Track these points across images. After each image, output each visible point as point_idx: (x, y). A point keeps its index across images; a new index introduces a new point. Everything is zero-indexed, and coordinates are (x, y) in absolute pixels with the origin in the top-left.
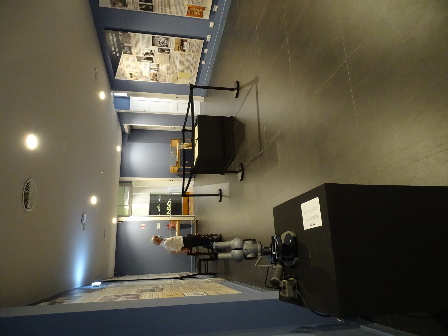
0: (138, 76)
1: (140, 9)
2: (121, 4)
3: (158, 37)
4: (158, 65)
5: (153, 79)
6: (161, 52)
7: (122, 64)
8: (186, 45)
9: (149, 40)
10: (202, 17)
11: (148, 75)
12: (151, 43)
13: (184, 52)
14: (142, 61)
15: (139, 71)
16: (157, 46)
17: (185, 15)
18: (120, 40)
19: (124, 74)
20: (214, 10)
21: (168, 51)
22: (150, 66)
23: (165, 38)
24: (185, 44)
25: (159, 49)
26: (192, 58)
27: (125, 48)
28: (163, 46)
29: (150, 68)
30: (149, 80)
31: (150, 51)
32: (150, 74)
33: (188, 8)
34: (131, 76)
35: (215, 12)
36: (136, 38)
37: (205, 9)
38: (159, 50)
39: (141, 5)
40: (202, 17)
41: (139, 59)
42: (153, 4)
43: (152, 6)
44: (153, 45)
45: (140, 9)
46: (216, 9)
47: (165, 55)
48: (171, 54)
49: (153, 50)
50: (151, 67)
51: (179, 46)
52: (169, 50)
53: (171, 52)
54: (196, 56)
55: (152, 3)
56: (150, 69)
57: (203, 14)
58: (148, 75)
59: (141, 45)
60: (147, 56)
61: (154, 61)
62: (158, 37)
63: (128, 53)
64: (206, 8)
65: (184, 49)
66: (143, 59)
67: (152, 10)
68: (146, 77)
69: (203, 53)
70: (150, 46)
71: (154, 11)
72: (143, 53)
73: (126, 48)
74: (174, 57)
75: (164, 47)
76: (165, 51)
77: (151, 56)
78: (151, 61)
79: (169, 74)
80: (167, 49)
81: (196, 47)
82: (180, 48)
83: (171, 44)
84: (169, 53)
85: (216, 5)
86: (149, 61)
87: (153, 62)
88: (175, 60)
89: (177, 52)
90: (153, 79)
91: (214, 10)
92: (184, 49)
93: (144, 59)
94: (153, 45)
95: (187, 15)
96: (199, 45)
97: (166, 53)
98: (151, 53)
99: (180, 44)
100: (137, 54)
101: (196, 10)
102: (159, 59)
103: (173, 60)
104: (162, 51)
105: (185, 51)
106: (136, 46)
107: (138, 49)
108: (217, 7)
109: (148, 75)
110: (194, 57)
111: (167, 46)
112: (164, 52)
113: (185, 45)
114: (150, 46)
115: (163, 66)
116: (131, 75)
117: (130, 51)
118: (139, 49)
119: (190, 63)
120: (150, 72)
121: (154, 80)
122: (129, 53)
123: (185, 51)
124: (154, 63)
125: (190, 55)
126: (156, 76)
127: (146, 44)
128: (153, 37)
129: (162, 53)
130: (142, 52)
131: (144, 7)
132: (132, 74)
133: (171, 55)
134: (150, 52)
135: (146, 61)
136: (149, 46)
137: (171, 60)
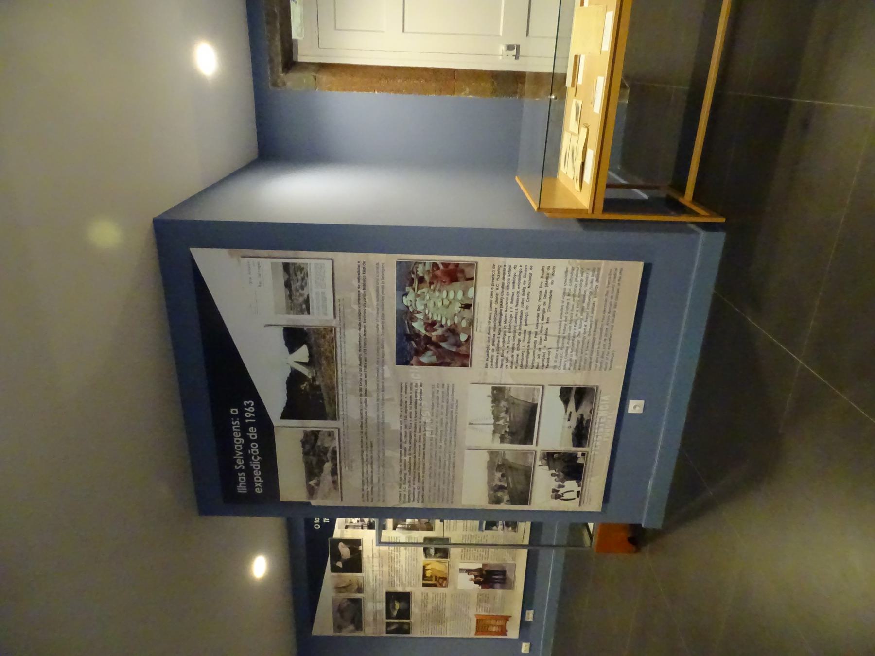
1: (388, 632)
2: (351, 627)
10: (506, 635)
17: (472, 634)
20: (527, 619)
33: (477, 620)
35: (530, 622)
37: (510, 619)
39: (388, 625)
40: (506, 635)
42: (412, 620)
43: (409, 624)
45: (388, 632)
46: (530, 616)
55: (408, 617)
57: (507, 629)
64: (510, 617)
67: (408, 632)
85: (531, 609)
91: (527, 619)
95: (475, 635)
101: (493, 622)
108: (532, 611)
131: (393, 627)
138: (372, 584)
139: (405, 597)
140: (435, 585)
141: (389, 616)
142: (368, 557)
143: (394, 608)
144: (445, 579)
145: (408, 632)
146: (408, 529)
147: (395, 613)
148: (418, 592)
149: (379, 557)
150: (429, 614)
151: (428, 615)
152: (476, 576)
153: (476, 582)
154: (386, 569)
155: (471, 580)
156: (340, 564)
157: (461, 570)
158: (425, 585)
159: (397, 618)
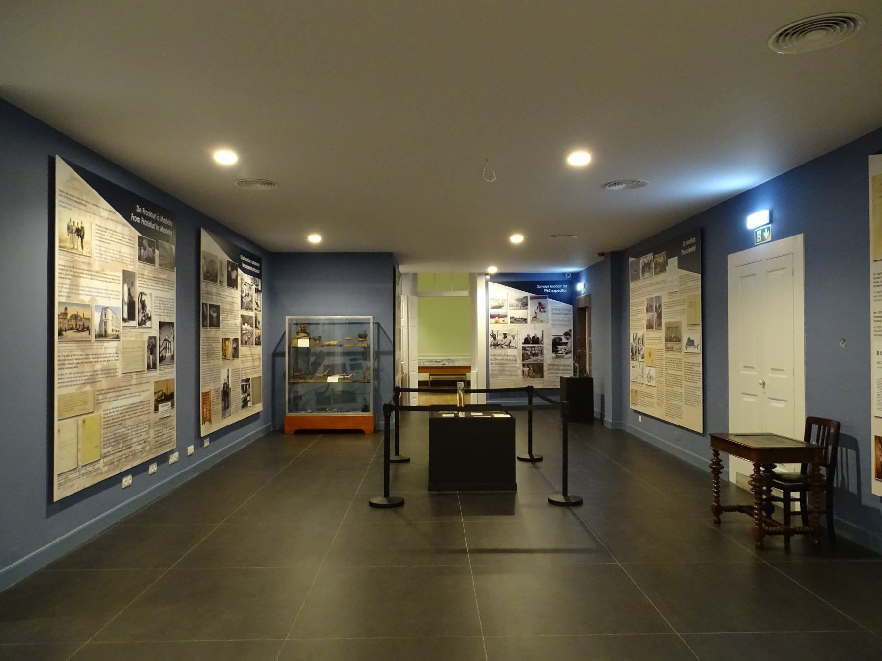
0: (77, 257)
1: (203, 303)
2: (205, 270)
3: (174, 338)
4: (117, 338)
5: (68, 317)
6: (149, 345)
7: (112, 217)
8: (166, 408)
9: (169, 314)
11: (82, 297)
12: (164, 319)
13: (153, 408)
14: (126, 285)
15: (96, 267)
16: (160, 333)
18: (165, 243)
19: (82, 207)
21: (152, 365)
22: (114, 310)
23: (173, 354)
24: (168, 405)
25: (155, 338)
26: (144, 436)
27: (150, 246)
28: (161, 350)
29: (108, 308)
30: (63, 300)
31: (150, 316)
32: (88, 306)
34: (74, 229)
36: (167, 281)
38: (153, 339)
39: (206, 304)
41: (129, 278)
42: (209, 329)
43: (206, 326)
44: (162, 324)
45: (203, 303)
47: (143, 355)
48: (148, 375)
49: (152, 324)
50: (110, 314)
51: (164, 391)
52: (155, 366)
53: (152, 373)
54: (148, 448)
56: (105, 309)
58: (86, 299)
59: (160, 294)
60: (138, 306)
61: (127, 324)
62: (174, 338)
63: (140, 249)
65: (160, 406)
66: (129, 290)
68: (74, 287)
69: (145, 466)
70: (159, 315)
71: (203, 329)
72: (143, 293)
73: (151, 249)
74: (141, 384)
75: (160, 352)
76: (151, 357)
77: (138, 316)
78: (126, 316)
79: (92, 380)
80: (156, 360)
81: (165, 436)
82: (160, 393)
83: (166, 370)
84: (149, 367)
86: (126, 307)
87: (124, 320)
88: (133, 389)
89: (153, 391)
90: (68, 317)
92: (160, 406)
93: (130, 294)
94: (162, 324)
96: (168, 442)
97: (149, 358)
98: (144, 316)
99: (166, 393)
100: (140, 276)
102: (133, 339)
103: (134, 382)
104: (152, 348)
105: (156, 409)
106: (156, 279)
107: (152, 281)
109: (82, 297)
110: (145, 442)
111: (162, 359)
112: (149, 353)
113: (166, 406)
114: (159, 315)
115: (116, 353)
116: (80, 232)
117: (145, 257)
118: (150, 284)
119: (131, 439)
120: (93, 308)
121: (66, 321)
122: (142, 254)
123: (156, 409)
124: (122, 324)
125: (149, 426)
126: (83, 331)
127: (161, 305)
128: (173, 324)
129: (148, 347)
130: (145, 293)
132: (82, 238)
133: (144, 375)
134: (147, 314)
135: (126, 299)
136: (158, 314)
137: (134, 377)
138: (223, 294)
139: (218, 325)
140: (223, 348)
141: (212, 306)
142: (231, 294)
143: (214, 312)
144: (225, 358)
145: (203, 326)
146: (241, 326)
147: (211, 313)
148: (218, 334)
149: (232, 302)
150: (211, 345)
151: (210, 344)
152: (226, 384)
153: (224, 384)
154: (228, 307)
155: (225, 380)
156: (230, 269)
157: (228, 370)
158: (223, 339)
159: (210, 314)
